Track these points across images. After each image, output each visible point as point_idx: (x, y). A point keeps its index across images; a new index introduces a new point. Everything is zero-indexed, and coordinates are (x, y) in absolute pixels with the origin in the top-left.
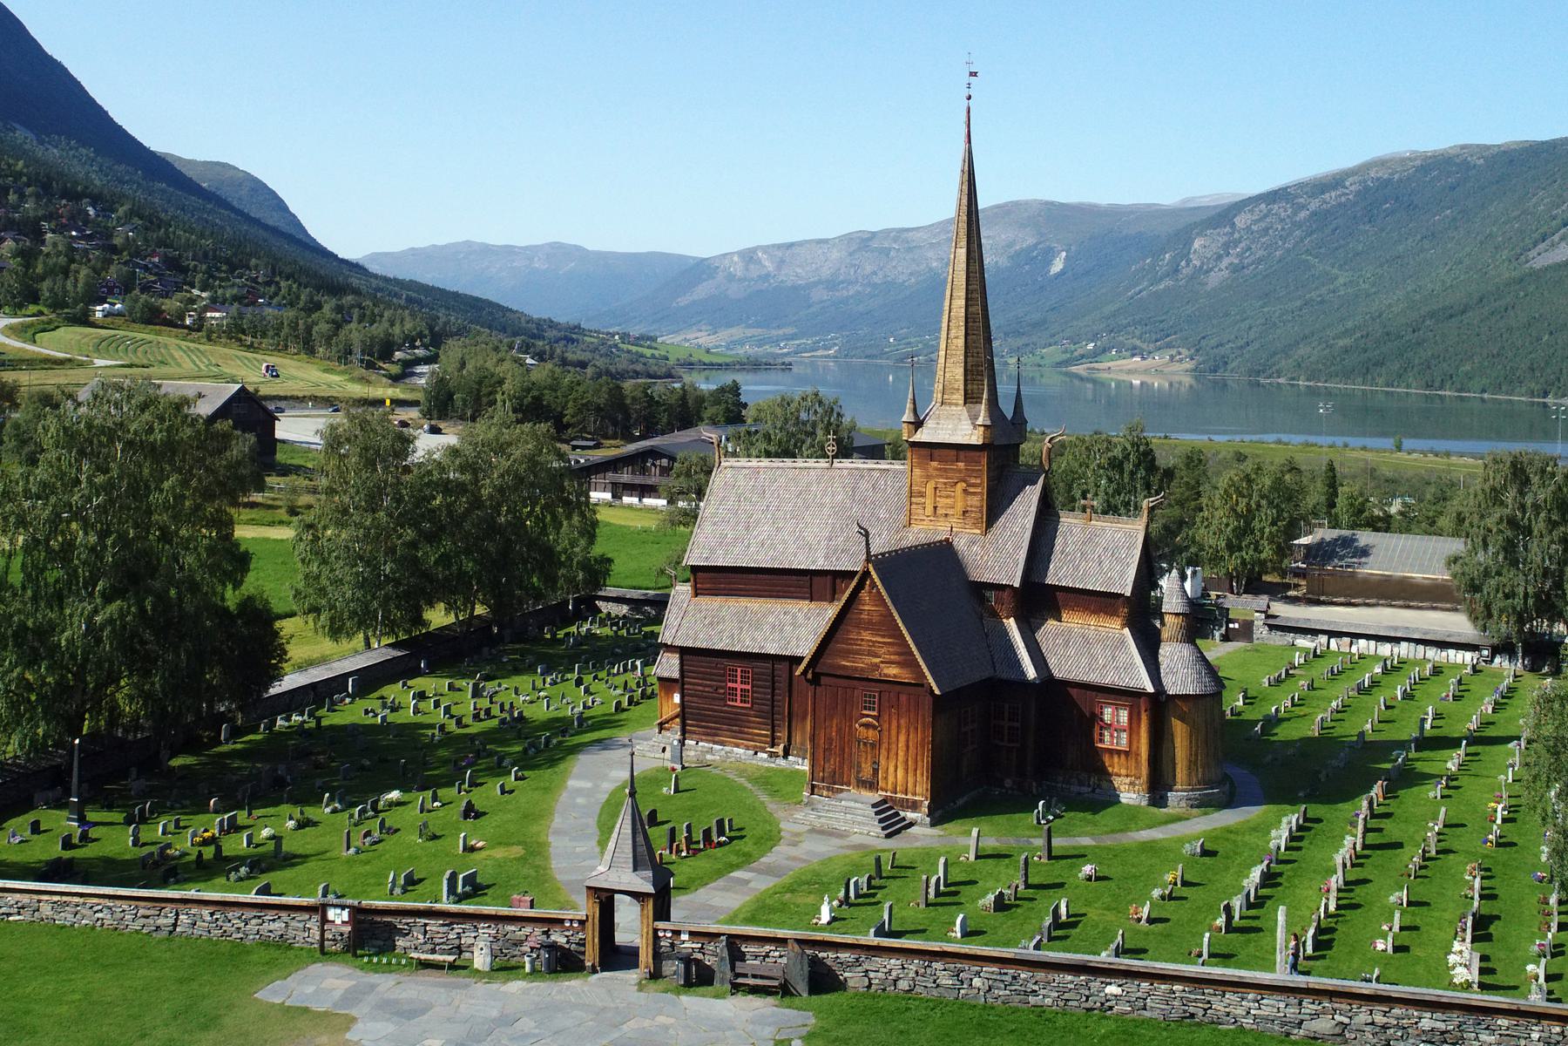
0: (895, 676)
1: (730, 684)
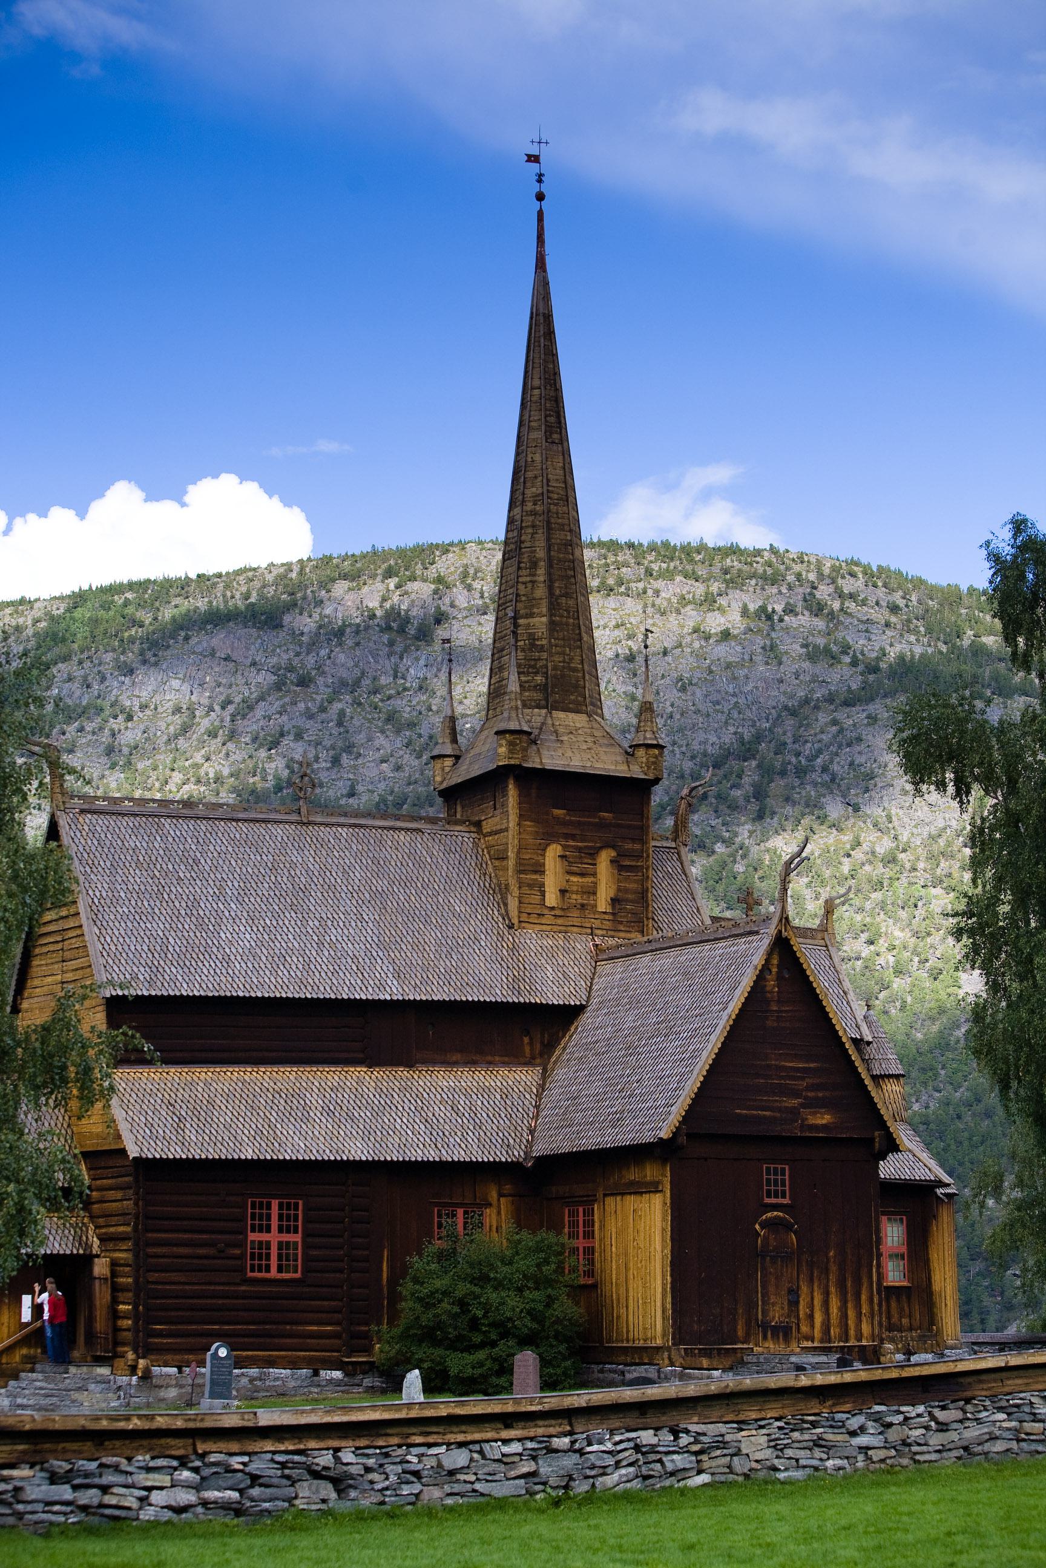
0: (825, 1127)
1: (253, 1237)
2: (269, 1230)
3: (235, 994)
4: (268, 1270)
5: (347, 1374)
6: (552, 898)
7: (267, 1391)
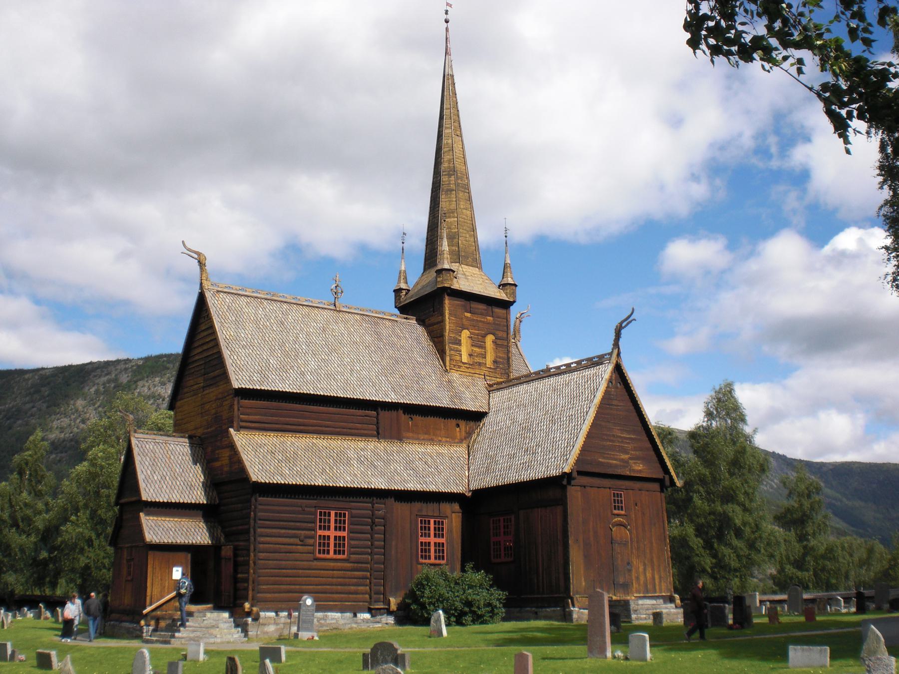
0: (640, 471)
1: (320, 532)
2: (329, 529)
3: (308, 392)
4: (328, 552)
5: (372, 616)
6: (465, 358)
7: (327, 626)
